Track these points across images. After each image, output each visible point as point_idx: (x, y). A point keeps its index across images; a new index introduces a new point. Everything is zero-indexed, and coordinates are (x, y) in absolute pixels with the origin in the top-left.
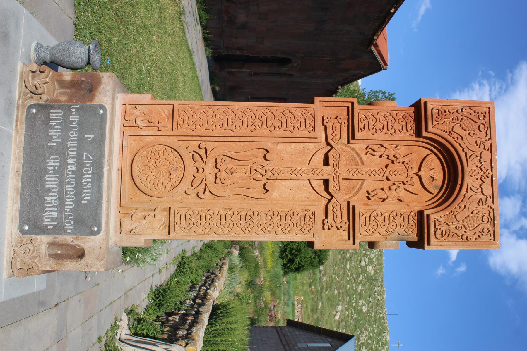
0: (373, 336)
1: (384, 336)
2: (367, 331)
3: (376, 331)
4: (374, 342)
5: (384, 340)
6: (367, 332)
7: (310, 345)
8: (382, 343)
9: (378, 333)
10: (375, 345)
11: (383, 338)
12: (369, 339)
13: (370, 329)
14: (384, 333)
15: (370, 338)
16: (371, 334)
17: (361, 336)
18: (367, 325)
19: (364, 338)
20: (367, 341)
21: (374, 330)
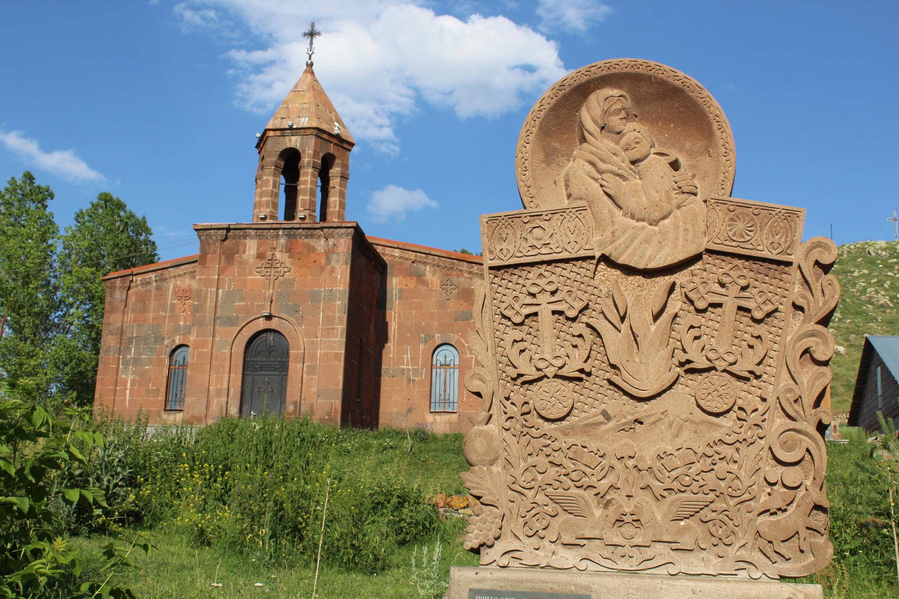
0: (877, 276)
1: (877, 253)
2: (865, 291)
3: (866, 272)
4: (889, 274)
5: (884, 253)
6: (868, 291)
7: (880, 393)
8: (890, 257)
9: (870, 266)
10: (895, 272)
11: (880, 255)
12: (883, 285)
13: (863, 284)
14: (869, 253)
15: (880, 284)
16: (873, 281)
17: (878, 301)
18: (855, 290)
19: (880, 295)
20: (886, 290)
21: (864, 275)
